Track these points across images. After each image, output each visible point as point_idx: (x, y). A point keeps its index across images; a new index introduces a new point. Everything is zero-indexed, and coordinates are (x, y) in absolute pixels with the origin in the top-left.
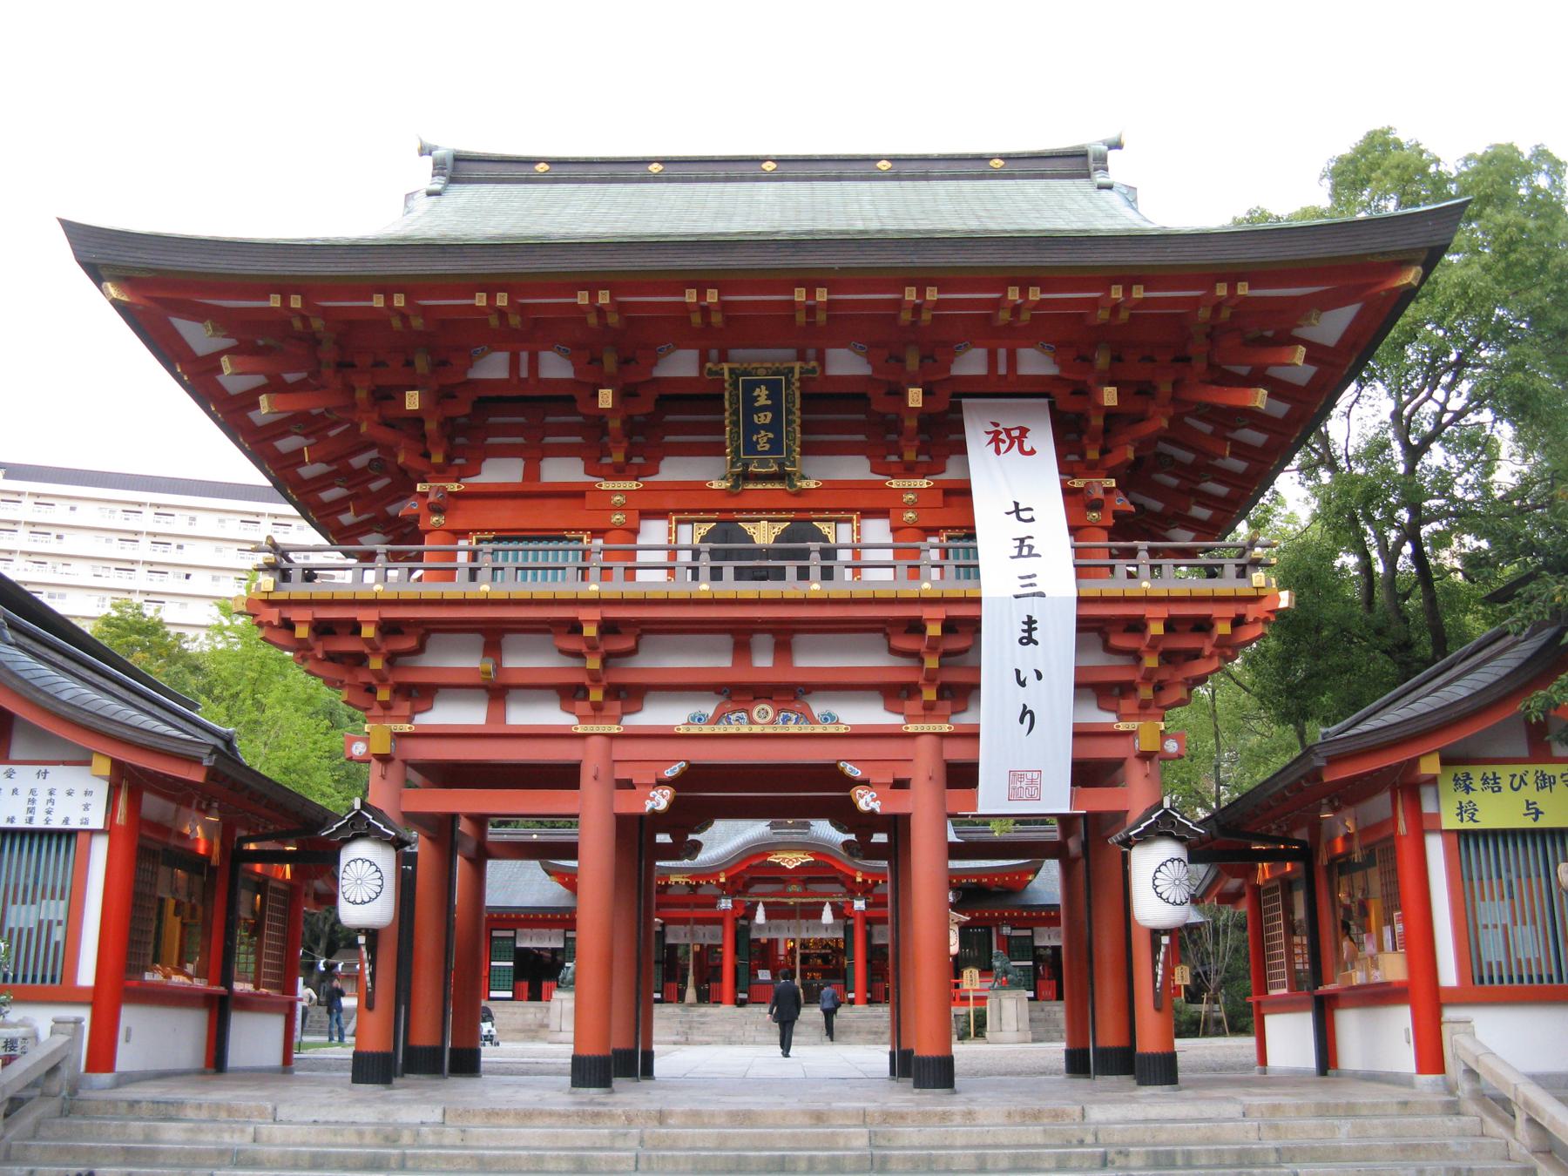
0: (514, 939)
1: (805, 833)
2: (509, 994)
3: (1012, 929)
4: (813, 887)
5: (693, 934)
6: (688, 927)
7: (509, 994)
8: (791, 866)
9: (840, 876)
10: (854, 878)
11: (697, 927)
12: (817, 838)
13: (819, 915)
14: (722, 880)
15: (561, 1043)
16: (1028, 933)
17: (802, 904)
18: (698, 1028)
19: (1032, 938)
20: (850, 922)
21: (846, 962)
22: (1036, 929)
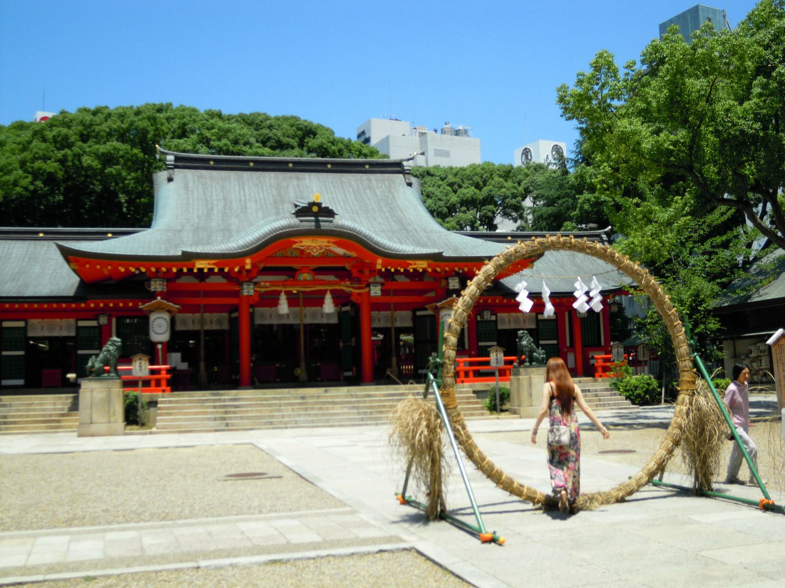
0: (25, 329)
1: (331, 222)
2: (21, 382)
3: (492, 314)
4: (317, 277)
5: (202, 321)
6: (198, 315)
7: (21, 382)
8: (316, 253)
9: (348, 266)
10: (375, 264)
11: (207, 315)
12: (342, 227)
13: (321, 303)
14: (248, 267)
15: (92, 435)
16: (493, 318)
17: (305, 293)
18: (235, 412)
19: (496, 322)
20: (347, 308)
21: (341, 344)
22: (499, 315)
